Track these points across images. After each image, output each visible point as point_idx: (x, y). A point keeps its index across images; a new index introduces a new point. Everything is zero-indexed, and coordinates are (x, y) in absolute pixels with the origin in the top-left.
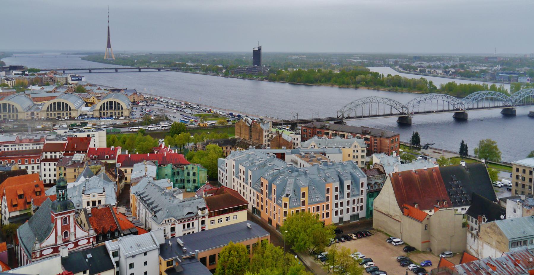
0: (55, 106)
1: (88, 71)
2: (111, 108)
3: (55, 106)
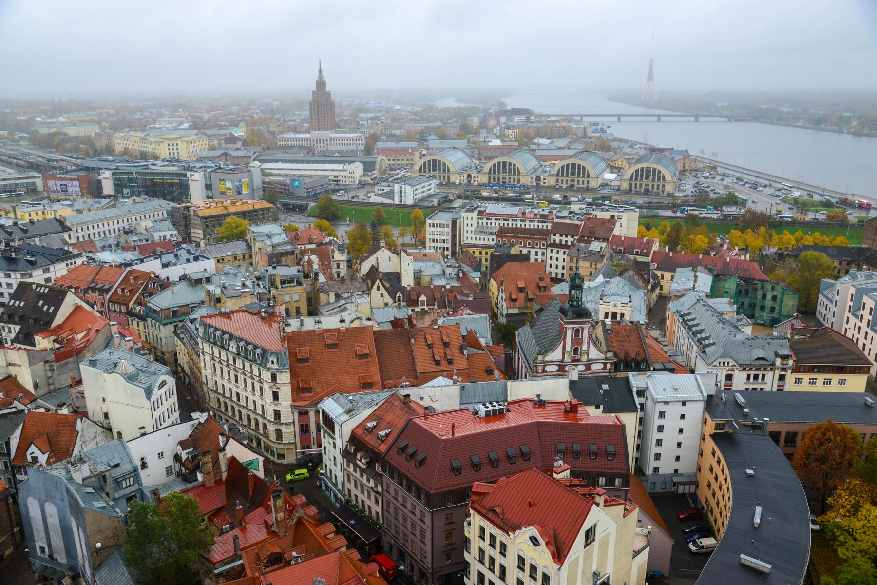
0: (429, 165)
1: (616, 119)
2: (434, 170)
3: (429, 165)
